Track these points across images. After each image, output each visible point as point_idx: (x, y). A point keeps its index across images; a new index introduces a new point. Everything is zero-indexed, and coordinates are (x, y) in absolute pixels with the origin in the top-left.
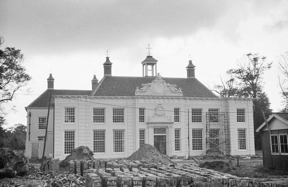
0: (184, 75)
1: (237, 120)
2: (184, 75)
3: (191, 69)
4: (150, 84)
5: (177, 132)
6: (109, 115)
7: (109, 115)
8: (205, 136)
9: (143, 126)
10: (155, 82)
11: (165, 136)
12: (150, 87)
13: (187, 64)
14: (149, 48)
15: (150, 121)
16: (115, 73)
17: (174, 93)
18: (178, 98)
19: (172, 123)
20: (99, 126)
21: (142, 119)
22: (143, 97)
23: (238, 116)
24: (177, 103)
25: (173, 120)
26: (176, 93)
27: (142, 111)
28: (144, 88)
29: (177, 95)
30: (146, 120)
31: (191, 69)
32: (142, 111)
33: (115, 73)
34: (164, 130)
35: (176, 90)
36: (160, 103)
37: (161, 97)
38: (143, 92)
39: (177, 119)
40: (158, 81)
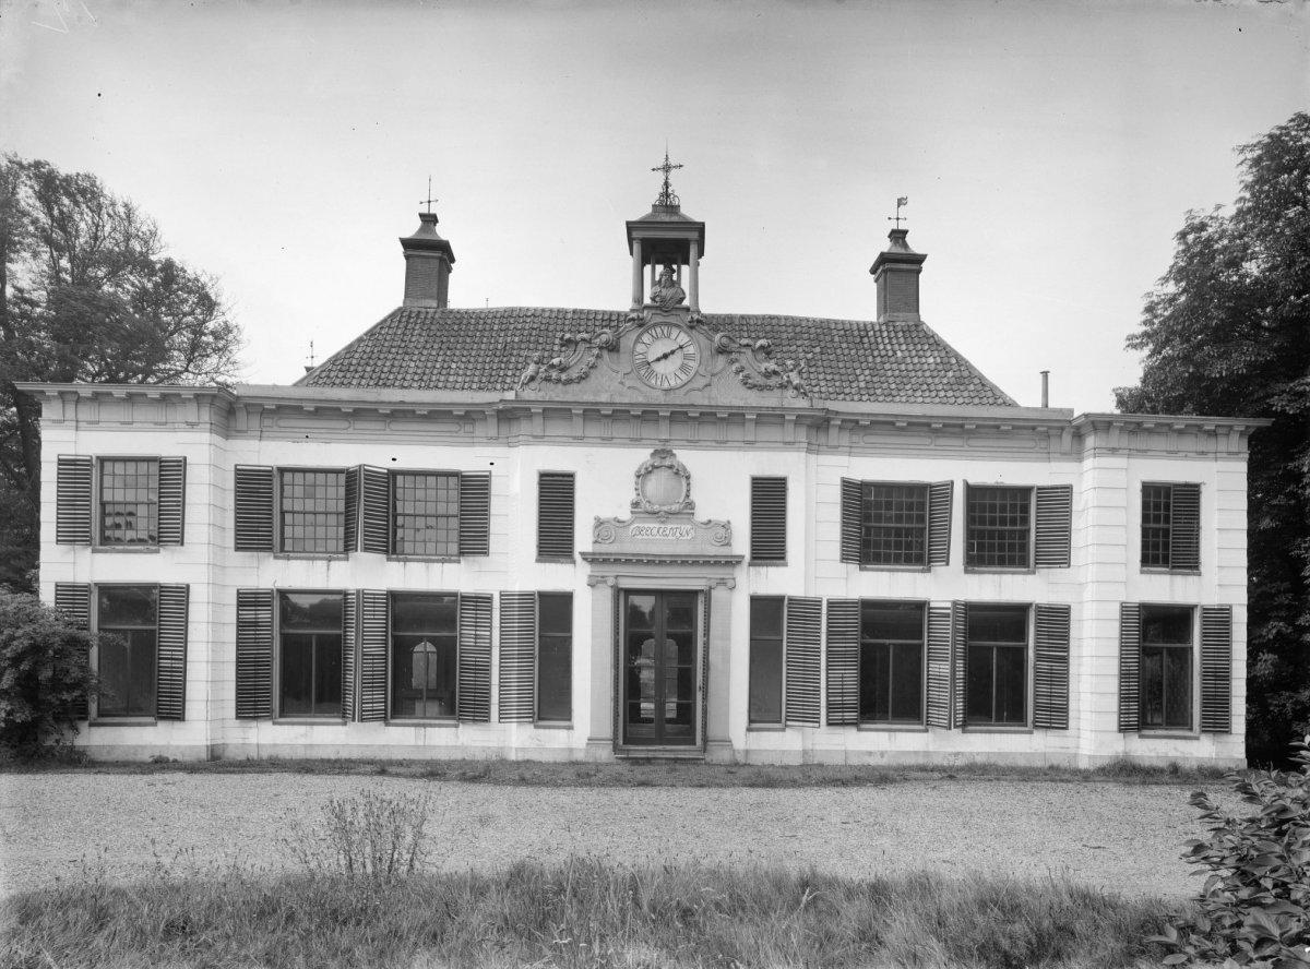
0: (859, 303)
2: (859, 303)
10: (640, 326)
12: (605, 354)
14: (667, 168)
15: (604, 548)
16: (466, 291)
17: (761, 388)
19: (732, 562)
25: (742, 545)
29: (770, 400)
30: (583, 540)
33: (466, 291)
35: (768, 374)
38: (569, 382)
40: (659, 319)
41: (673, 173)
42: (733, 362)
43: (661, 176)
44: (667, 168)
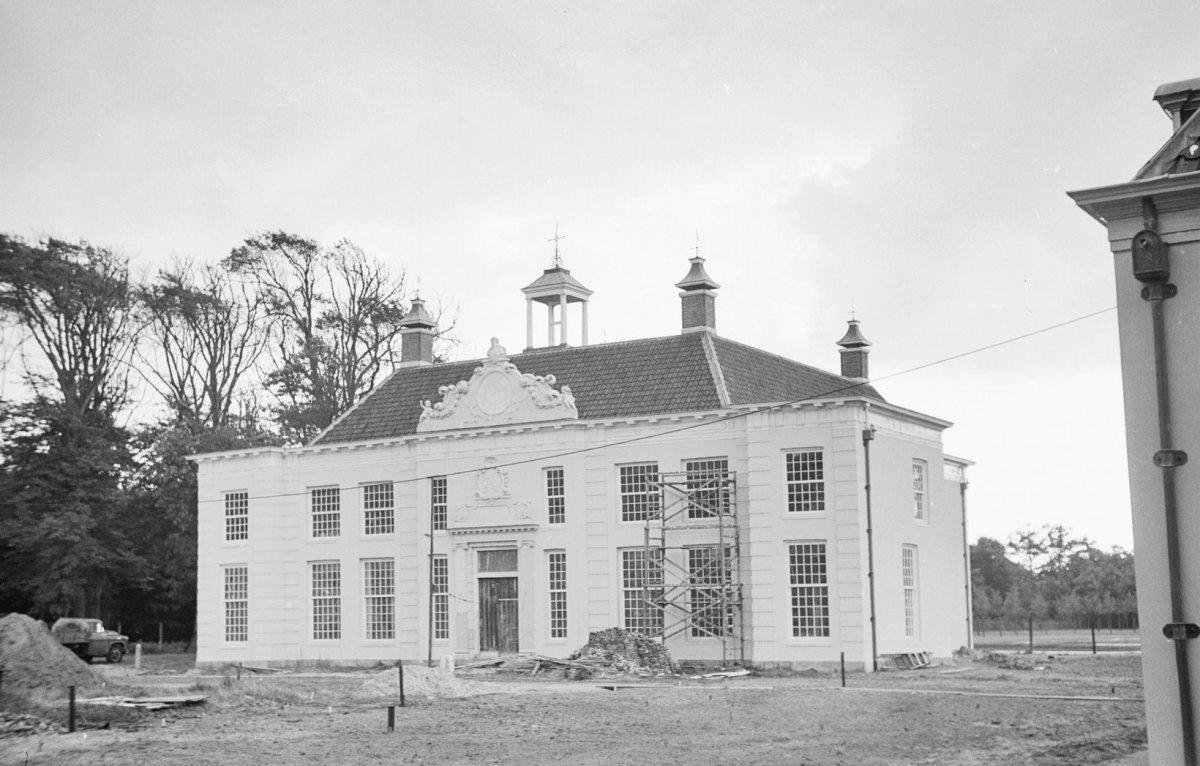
0: (668, 323)
1: (787, 503)
3: (697, 294)
4: (463, 384)
5: (558, 562)
6: (352, 509)
7: (352, 509)
8: (676, 577)
9: (443, 543)
11: (517, 578)
13: (682, 271)
14: (556, 239)
18: (566, 425)
20: (326, 549)
21: (439, 517)
22: (449, 435)
23: (816, 481)
24: (552, 447)
26: (551, 407)
27: (439, 486)
28: (445, 405)
31: (697, 294)
32: (439, 486)
34: (510, 556)
36: (492, 454)
37: (427, 436)
39: (557, 511)
41: (560, 241)
42: (530, 392)
43: (553, 243)
44: (556, 239)
